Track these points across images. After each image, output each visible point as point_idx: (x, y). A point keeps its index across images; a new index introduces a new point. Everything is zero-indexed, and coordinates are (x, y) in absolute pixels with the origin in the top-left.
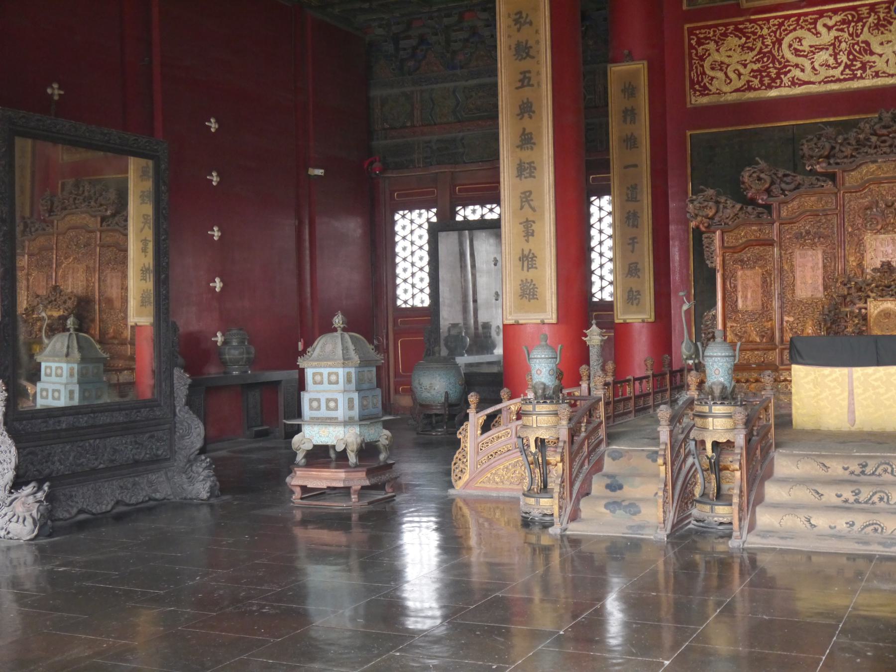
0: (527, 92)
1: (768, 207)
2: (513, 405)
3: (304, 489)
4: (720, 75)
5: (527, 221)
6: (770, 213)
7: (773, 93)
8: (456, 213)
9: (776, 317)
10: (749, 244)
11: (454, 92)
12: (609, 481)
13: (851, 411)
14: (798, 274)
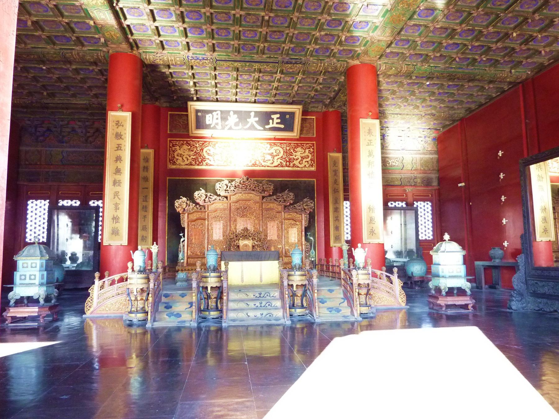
0: (119, 153)
2: (117, 277)
3: (13, 318)
4: (180, 158)
5: (116, 203)
8: (59, 203)
11: (62, 152)
12: (166, 305)
13: (242, 278)
14: (214, 231)
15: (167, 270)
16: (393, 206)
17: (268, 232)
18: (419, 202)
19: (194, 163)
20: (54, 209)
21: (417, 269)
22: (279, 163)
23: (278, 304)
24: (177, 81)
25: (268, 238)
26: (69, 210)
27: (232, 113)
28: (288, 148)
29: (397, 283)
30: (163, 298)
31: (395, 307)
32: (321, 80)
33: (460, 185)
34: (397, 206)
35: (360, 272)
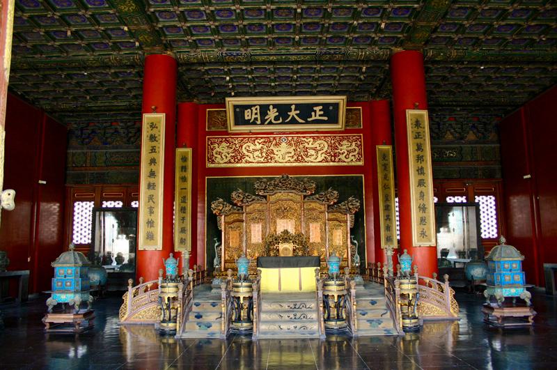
1: (242, 207)
2: (149, 284)
3: (51, 324)
4: (219, 156)
6: (242, 209)
7: (239, 165)
9: (244, 250)
10: (234, 221)
12: (196, 314)
15: (205, 275)
16: (452, 201)
17: (311, 234)
18: (481, 197)
19: (232, 160)
20: (98, 210)
21: (477, 272)
22: (323, 157)
23: (314, 316)
24: (213, 78)
25: (311, 241)
26: (114, 211)
27: (271, 107)
28: (333, 142)
29: (449, 292)
30: (194, 306)
31: (445, 317)
32: (364, 70)
33: (525, 177)
34: (457, 201)
35: (405, 281)
